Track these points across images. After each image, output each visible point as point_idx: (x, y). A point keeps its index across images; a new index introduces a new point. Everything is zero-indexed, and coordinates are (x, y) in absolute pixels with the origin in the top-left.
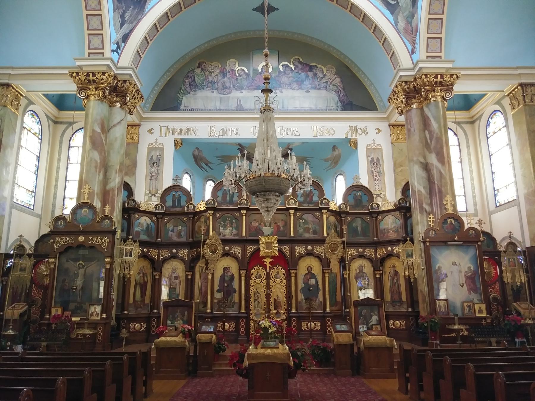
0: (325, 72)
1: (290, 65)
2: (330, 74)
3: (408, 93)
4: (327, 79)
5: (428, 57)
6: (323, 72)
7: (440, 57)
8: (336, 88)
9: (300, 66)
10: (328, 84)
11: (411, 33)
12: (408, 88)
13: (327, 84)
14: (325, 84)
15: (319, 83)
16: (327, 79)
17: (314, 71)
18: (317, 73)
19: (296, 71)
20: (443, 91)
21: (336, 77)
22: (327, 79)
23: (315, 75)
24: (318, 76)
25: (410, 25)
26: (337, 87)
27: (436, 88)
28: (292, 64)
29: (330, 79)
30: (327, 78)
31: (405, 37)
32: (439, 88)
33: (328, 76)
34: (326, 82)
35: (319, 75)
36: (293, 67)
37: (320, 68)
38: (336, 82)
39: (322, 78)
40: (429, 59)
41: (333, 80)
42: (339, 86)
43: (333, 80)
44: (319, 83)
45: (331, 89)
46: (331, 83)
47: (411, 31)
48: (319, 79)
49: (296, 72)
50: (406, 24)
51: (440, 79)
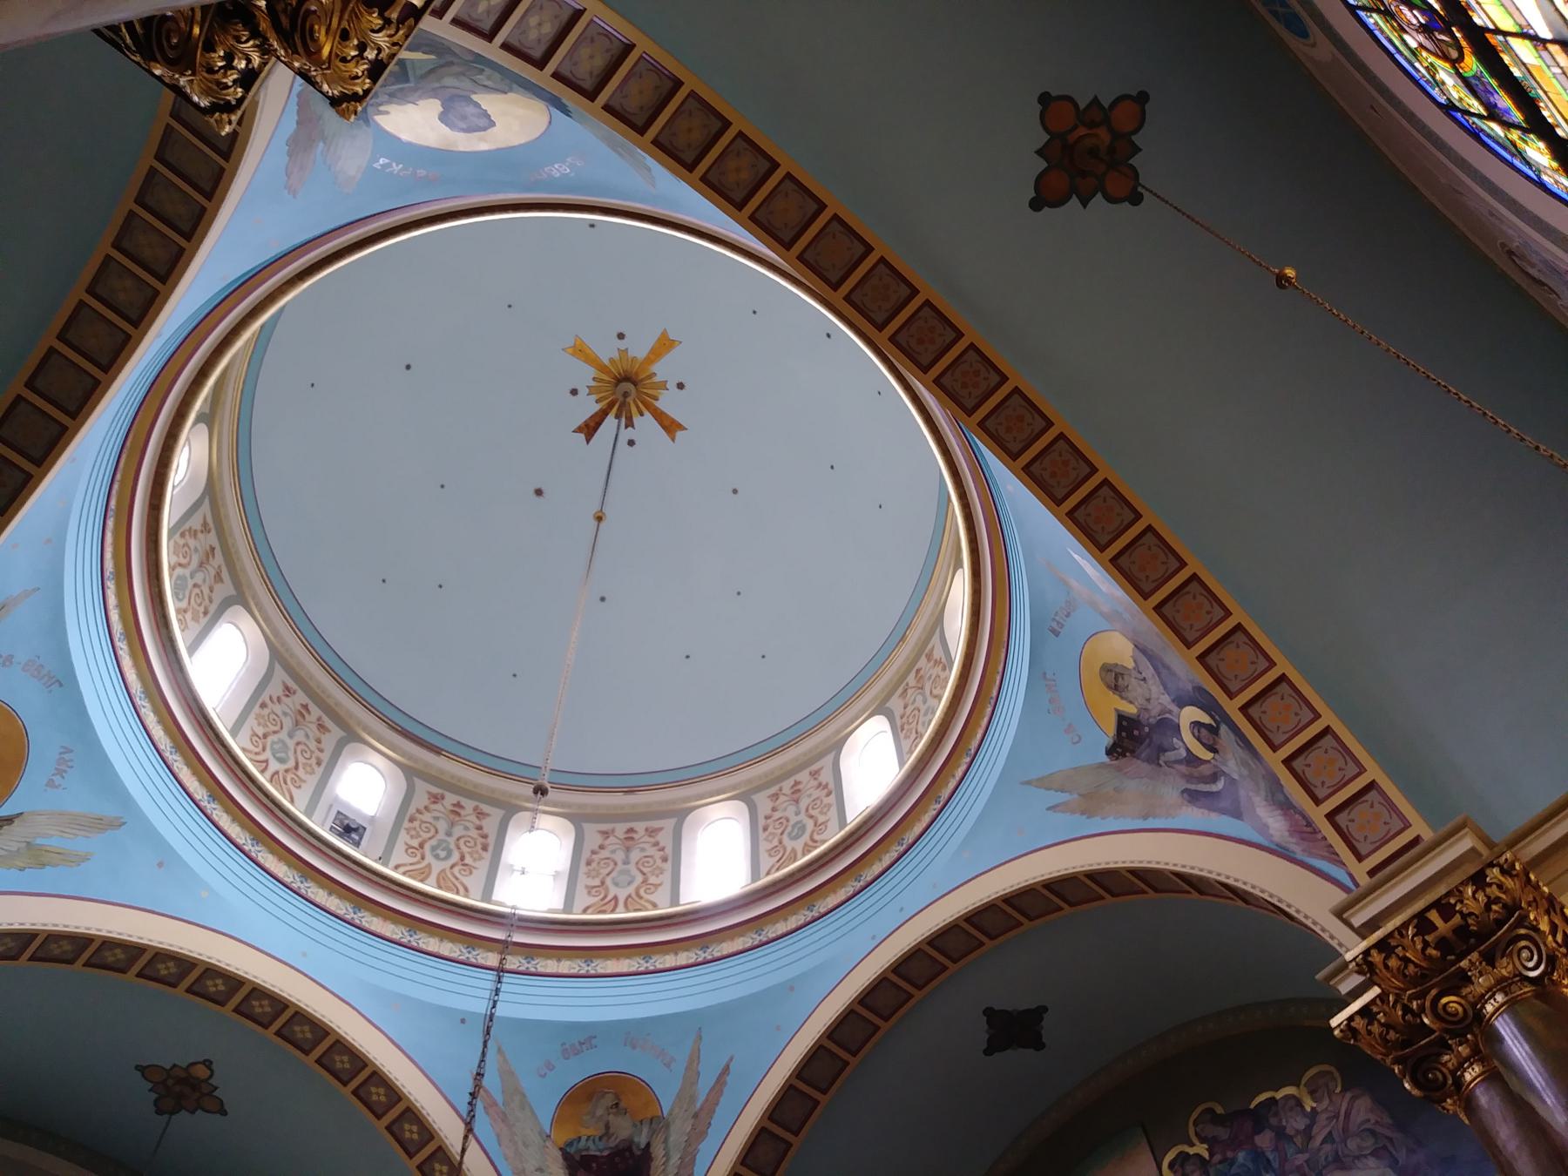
0: (1309, 1104)
1: (1191, 1151)
2: (1326, 1102)
3: (1405, 1044)
4: (1325, 1123)
5: (1372, 873)
6: (1302, 1107)
7: (1416, 840)
8: (1369, 1143)
9: (1223, 1133)
10: (1337, 1139)
11: (1309, 829)
12: (1388, 1026)
13: (1333, 1142)
14: (1328, 1147)
15: (1306, 1156)
16: (1324, 1127)
17: (1273, 1121)
18: (1284, 1124)
19: (1217, 1158)
20: (1498, 954)
21: (1354, 1098)
22: (1325, 1123)
23: (1281, 1134)
24: (1292, 1133)
25: (1292, 811)
26: (1373, 1132)
27: (1464, 964)
28: (1195, 1140)
29: (1337, 1116)
30: (1322, 1118)
31: (1311, 855)
32: (1475, 956)
33: (1322, 1112)
34: (1329, 1138)
35: (1295, 1124)
36: (1201, 1149)
37: (1287, 1097)
38: (1362, 1117)
39: (1307, 1133)
40: (1380, 875)
41: (1348, 1114)
42: (1377, 1122)
43: (1348, 1114)
44: (1306, 1156)
45: (1357, 1153)
46: (1345, 1130)
47: (1306, 826)
48: (1299, 1140)
49: (1220, 1162)
50: (1285, 815)
51: (1446, 921)
